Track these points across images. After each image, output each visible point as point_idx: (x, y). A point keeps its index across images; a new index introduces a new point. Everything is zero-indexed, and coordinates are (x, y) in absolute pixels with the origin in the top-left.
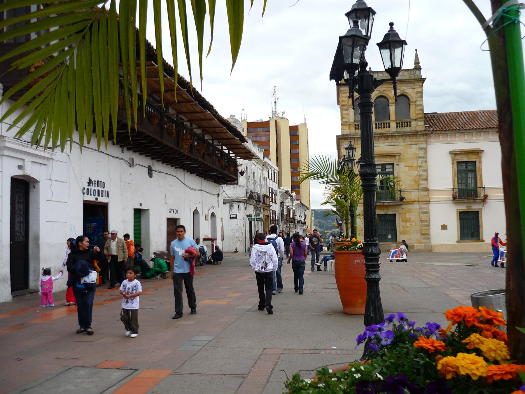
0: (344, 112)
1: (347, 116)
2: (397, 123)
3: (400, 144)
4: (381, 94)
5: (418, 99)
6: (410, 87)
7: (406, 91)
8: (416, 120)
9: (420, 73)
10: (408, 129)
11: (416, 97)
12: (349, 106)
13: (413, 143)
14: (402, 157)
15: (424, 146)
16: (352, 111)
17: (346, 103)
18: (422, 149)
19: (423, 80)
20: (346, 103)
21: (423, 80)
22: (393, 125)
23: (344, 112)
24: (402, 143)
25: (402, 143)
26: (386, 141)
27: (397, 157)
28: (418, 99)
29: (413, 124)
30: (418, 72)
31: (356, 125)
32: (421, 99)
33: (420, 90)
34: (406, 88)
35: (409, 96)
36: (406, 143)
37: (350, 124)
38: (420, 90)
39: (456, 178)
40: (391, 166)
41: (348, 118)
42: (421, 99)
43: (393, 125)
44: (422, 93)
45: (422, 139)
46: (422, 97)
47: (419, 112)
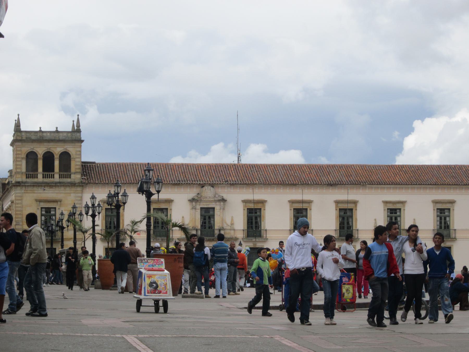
0: (18, 163)
1: (20, 167)
2: (60, 175)
3: (61, 192)
4: (49, 150)
5: (77, 156)
6: (71, 146)
7: (68, 149)
8: (75, 173)
9: (80, 135)
10: (69, 180)
11: (76, 154)
12: (22, 158)
13: (72, 192)
14: (62, 203)
15: (80, 195)
16: (24, 163)
17: (20, 156)
18: (79, 197)
19: (82, 141)
20: (20, 156)
21: (82, 141)
22: (57, 176)
23: (18, 163)
24: (63, 192)
25: (63, 192)
26: (51, 189)
27: (59, 203)
28: (77, 156)
29: (73, 176)
30: (78, 134)
31: (27, 175)
32: (79, 156)
33: (79, 149)
34: (68, 146)
35: (71, 154)
36: (66, 192)
37: (22, 173)
38: (79, 149)
39: (104, 221)
40: (54, 210)
41: (21, 168)
42: (79, 156)
43: (57, 176)
44: (80, 151)
45: (79, 189)
46: (80, 155)
47: (77, 167)
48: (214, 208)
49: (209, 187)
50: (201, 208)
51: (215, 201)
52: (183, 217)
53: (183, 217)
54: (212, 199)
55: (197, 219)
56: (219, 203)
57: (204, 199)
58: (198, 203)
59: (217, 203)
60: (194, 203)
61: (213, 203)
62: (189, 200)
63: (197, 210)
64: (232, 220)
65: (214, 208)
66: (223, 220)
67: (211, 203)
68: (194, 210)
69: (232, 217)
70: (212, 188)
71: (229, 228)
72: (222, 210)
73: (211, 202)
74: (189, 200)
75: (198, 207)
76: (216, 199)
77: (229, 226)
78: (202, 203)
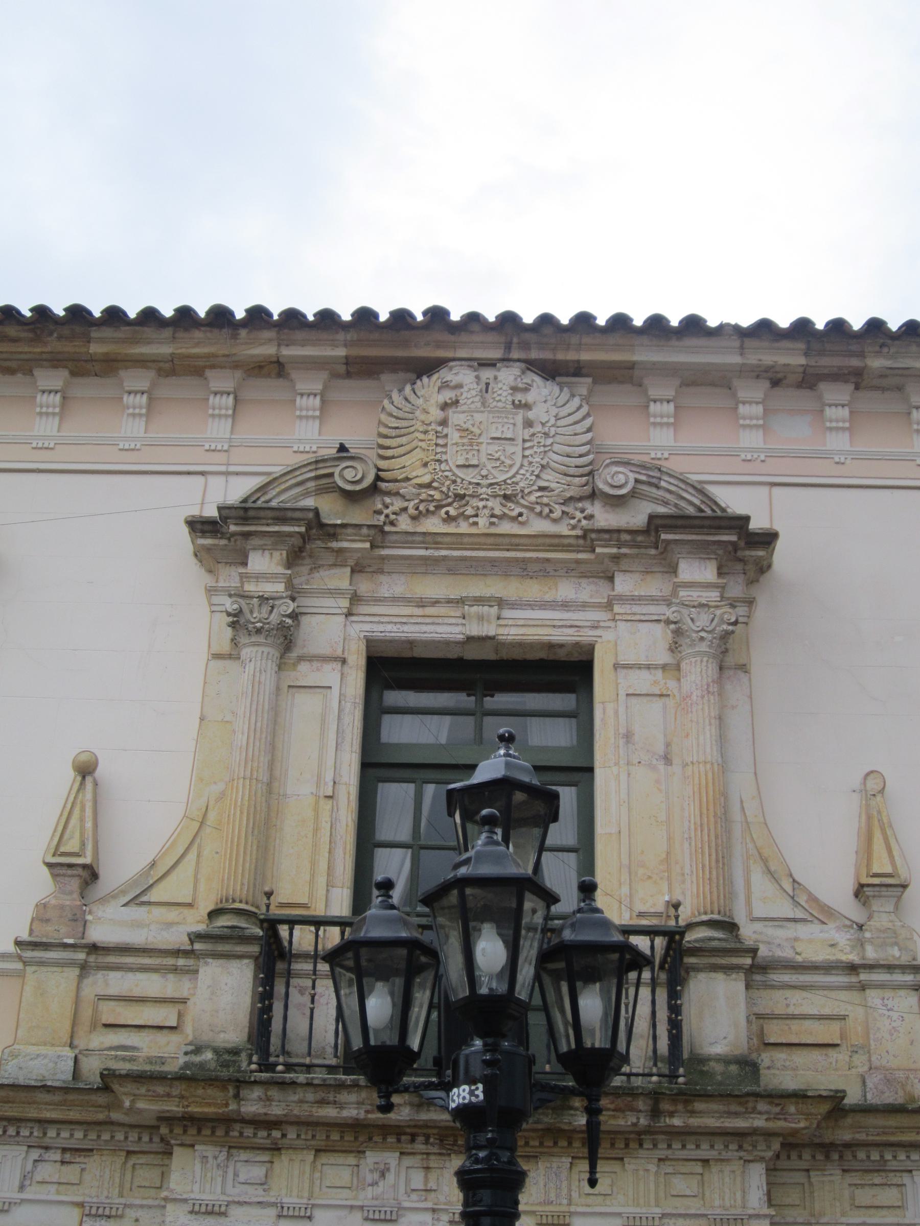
48: (566, 673)
49: (508, 376)
50: (393, 671)
51: (599, 554)
52: (85, 770)
53: (85, 770)
54: (540, 526)
55: (300, 789)
56: (655, 586)
57: (433, 525)
58: (340, 579)
59: (624, 584)
60: (264, 563)
61: (566, 590)
62: (199, 526)
63: (306, 674)
64: (875, 826)
65: (566, 673)
66: (722, 827)
67: (533, 590)
68: (258, 656)
69: (873, 792)
70: (542, 391)
71: (817, 942)
72: (698, 671)
73: (530, 560)
74: (199, 526)
75: (339, 633)
76: (604, 518)
77: (824, 913)
78: (393, 585)
